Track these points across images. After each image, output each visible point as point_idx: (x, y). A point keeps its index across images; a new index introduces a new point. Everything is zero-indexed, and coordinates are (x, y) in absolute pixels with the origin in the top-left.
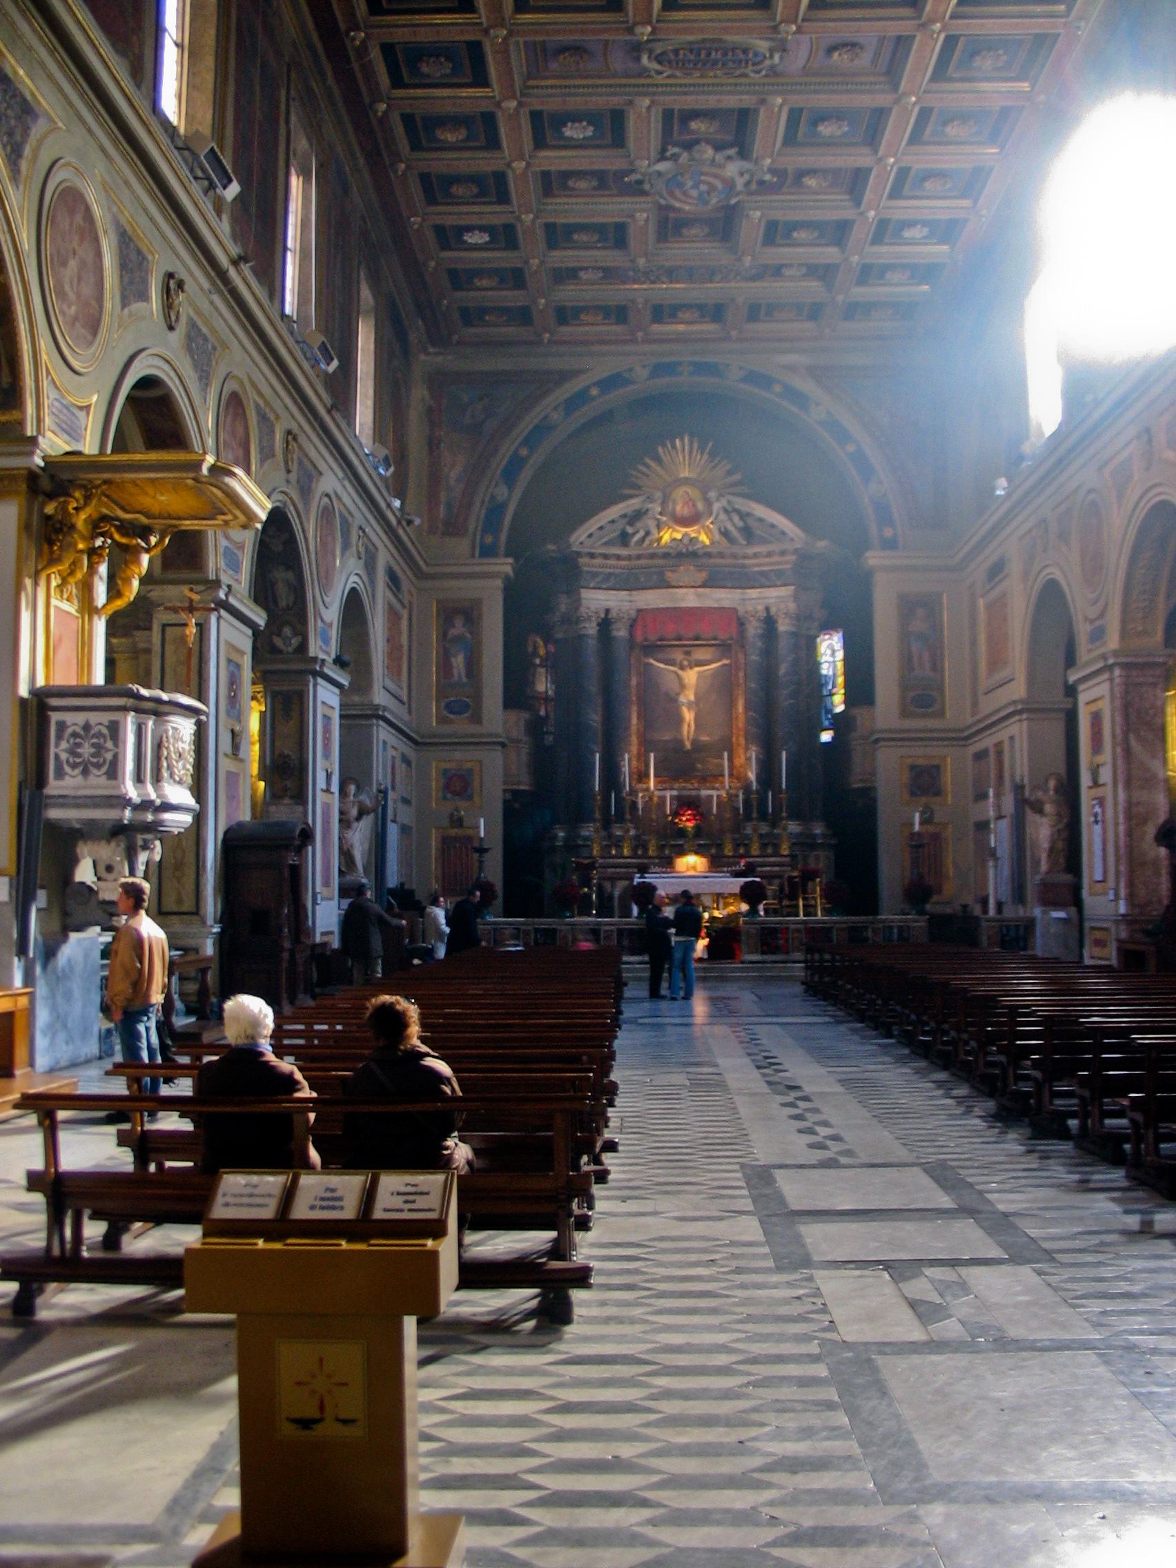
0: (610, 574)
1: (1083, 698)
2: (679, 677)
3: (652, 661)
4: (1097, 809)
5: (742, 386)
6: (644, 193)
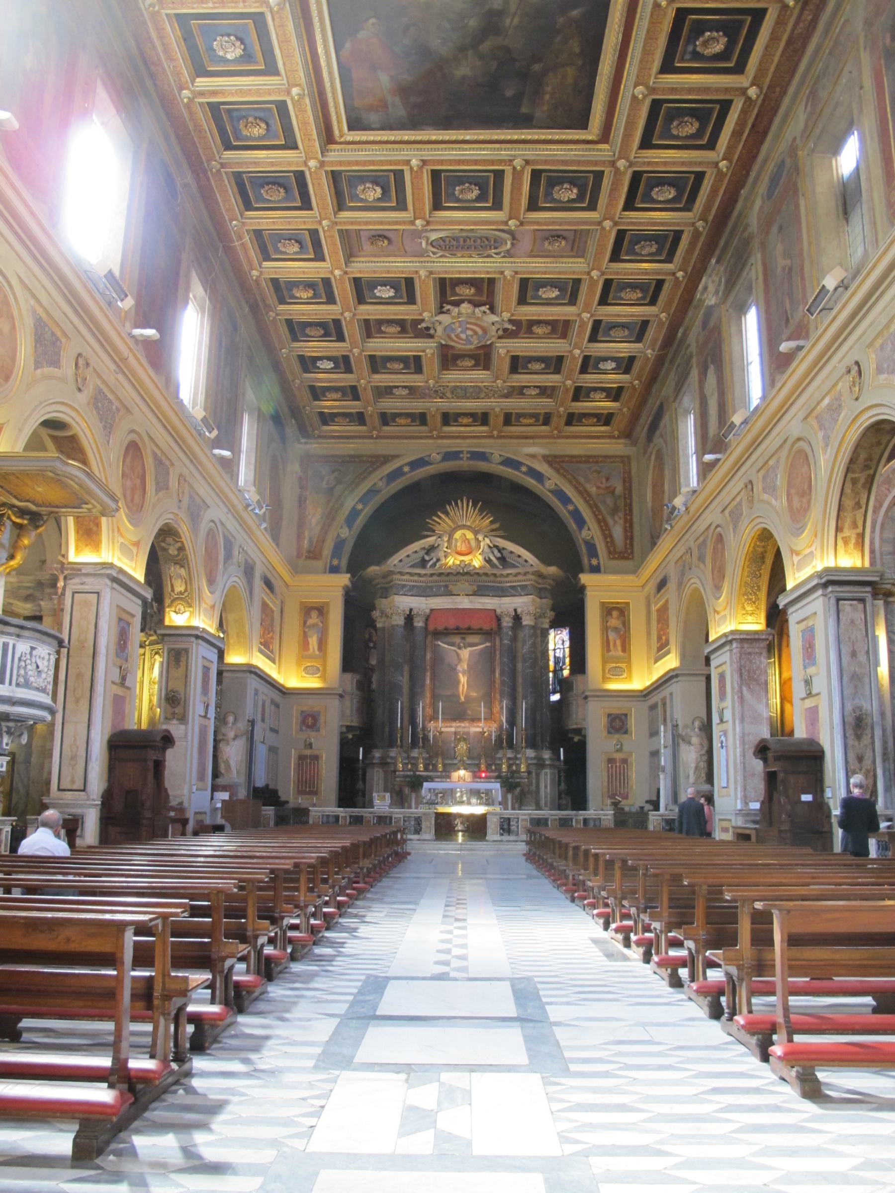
0: (414, 586)
1: (713, 664)
2: (457, 653)
3: (440, 643)
4: (723, 738)
5: (501, 467)
6: (432, 336)
